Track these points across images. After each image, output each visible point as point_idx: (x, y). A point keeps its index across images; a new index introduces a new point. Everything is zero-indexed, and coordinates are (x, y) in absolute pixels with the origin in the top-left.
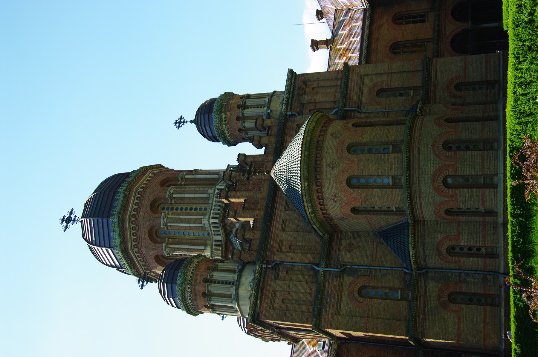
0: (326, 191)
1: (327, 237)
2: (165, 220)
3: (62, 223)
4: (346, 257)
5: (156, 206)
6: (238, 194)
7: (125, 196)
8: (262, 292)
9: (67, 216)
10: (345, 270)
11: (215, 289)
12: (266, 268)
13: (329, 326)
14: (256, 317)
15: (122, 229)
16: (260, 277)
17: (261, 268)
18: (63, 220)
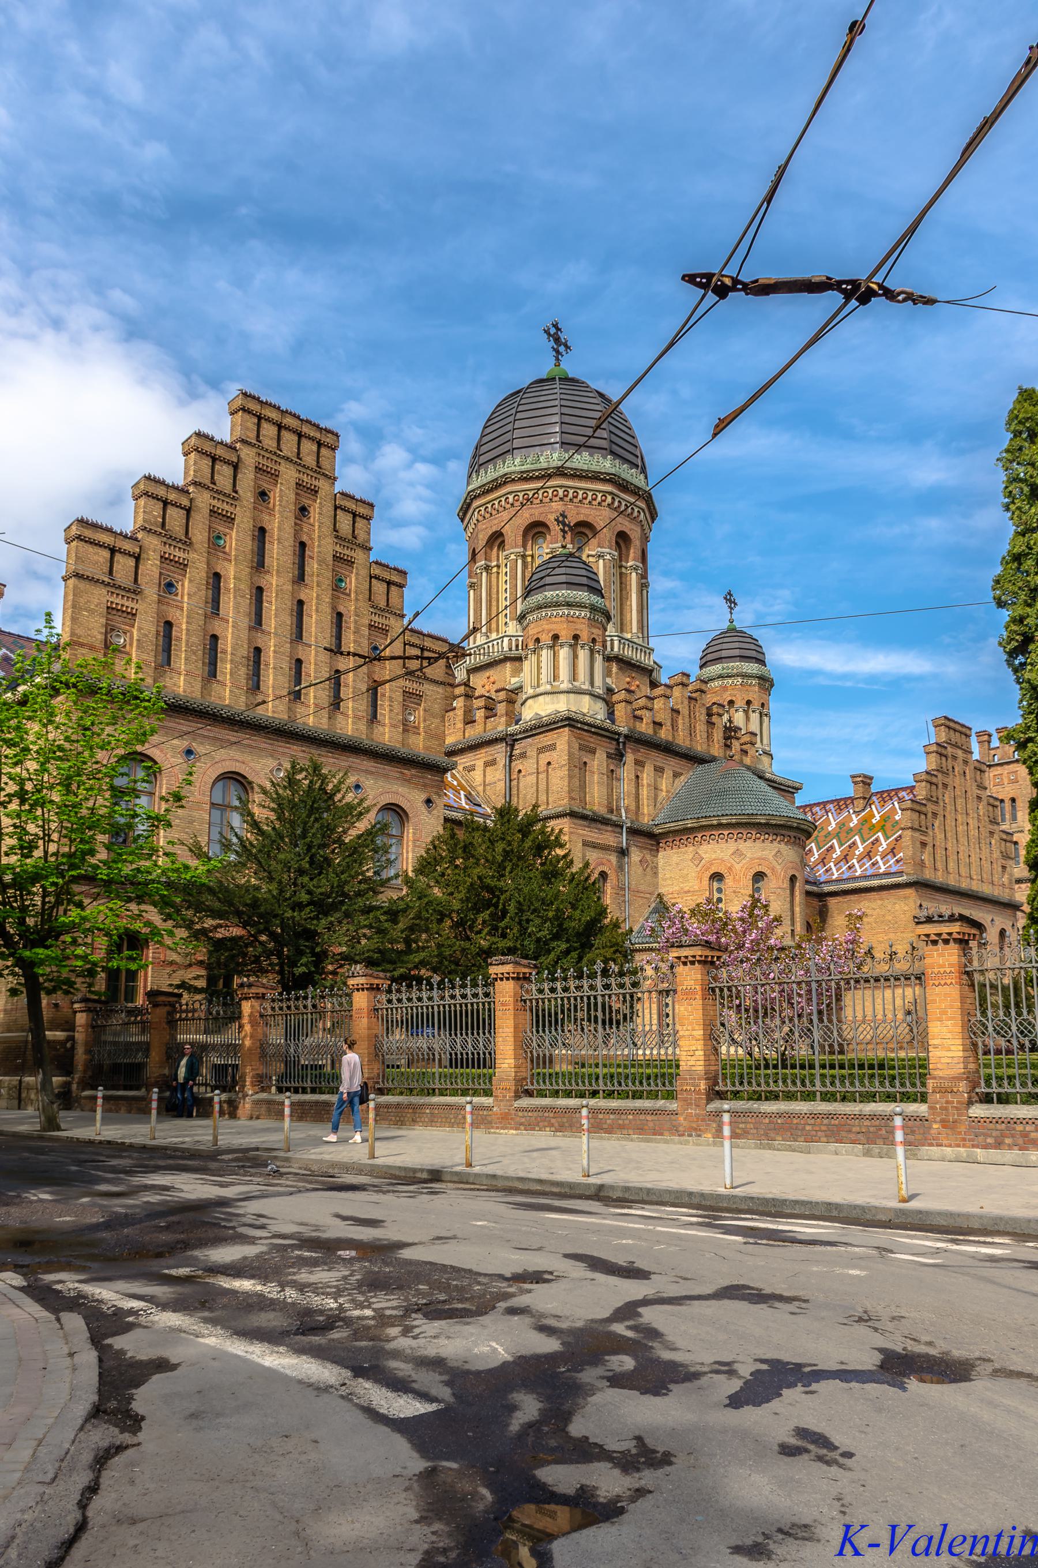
0: (749, 843)
1: (657, 831)
2: (608, 557)
3: (554, 326)
4: (635, 855)
5: (622, 539)
6: (686, 702)
7: (639, 488)
8: (594, 733)
9: (563, 336)
10: (623, 853)
11: (583, 655)
12: (617, 740)
13: (572, 830)
14: (572, 723)
15: (595, 477)
16: (612, 732)
17: (619, 734)
18: (558, 329)
